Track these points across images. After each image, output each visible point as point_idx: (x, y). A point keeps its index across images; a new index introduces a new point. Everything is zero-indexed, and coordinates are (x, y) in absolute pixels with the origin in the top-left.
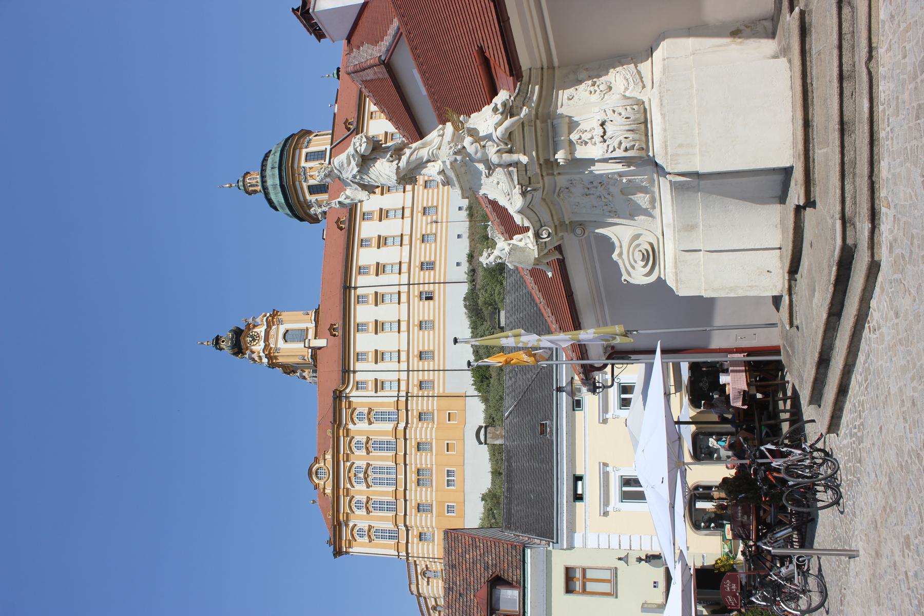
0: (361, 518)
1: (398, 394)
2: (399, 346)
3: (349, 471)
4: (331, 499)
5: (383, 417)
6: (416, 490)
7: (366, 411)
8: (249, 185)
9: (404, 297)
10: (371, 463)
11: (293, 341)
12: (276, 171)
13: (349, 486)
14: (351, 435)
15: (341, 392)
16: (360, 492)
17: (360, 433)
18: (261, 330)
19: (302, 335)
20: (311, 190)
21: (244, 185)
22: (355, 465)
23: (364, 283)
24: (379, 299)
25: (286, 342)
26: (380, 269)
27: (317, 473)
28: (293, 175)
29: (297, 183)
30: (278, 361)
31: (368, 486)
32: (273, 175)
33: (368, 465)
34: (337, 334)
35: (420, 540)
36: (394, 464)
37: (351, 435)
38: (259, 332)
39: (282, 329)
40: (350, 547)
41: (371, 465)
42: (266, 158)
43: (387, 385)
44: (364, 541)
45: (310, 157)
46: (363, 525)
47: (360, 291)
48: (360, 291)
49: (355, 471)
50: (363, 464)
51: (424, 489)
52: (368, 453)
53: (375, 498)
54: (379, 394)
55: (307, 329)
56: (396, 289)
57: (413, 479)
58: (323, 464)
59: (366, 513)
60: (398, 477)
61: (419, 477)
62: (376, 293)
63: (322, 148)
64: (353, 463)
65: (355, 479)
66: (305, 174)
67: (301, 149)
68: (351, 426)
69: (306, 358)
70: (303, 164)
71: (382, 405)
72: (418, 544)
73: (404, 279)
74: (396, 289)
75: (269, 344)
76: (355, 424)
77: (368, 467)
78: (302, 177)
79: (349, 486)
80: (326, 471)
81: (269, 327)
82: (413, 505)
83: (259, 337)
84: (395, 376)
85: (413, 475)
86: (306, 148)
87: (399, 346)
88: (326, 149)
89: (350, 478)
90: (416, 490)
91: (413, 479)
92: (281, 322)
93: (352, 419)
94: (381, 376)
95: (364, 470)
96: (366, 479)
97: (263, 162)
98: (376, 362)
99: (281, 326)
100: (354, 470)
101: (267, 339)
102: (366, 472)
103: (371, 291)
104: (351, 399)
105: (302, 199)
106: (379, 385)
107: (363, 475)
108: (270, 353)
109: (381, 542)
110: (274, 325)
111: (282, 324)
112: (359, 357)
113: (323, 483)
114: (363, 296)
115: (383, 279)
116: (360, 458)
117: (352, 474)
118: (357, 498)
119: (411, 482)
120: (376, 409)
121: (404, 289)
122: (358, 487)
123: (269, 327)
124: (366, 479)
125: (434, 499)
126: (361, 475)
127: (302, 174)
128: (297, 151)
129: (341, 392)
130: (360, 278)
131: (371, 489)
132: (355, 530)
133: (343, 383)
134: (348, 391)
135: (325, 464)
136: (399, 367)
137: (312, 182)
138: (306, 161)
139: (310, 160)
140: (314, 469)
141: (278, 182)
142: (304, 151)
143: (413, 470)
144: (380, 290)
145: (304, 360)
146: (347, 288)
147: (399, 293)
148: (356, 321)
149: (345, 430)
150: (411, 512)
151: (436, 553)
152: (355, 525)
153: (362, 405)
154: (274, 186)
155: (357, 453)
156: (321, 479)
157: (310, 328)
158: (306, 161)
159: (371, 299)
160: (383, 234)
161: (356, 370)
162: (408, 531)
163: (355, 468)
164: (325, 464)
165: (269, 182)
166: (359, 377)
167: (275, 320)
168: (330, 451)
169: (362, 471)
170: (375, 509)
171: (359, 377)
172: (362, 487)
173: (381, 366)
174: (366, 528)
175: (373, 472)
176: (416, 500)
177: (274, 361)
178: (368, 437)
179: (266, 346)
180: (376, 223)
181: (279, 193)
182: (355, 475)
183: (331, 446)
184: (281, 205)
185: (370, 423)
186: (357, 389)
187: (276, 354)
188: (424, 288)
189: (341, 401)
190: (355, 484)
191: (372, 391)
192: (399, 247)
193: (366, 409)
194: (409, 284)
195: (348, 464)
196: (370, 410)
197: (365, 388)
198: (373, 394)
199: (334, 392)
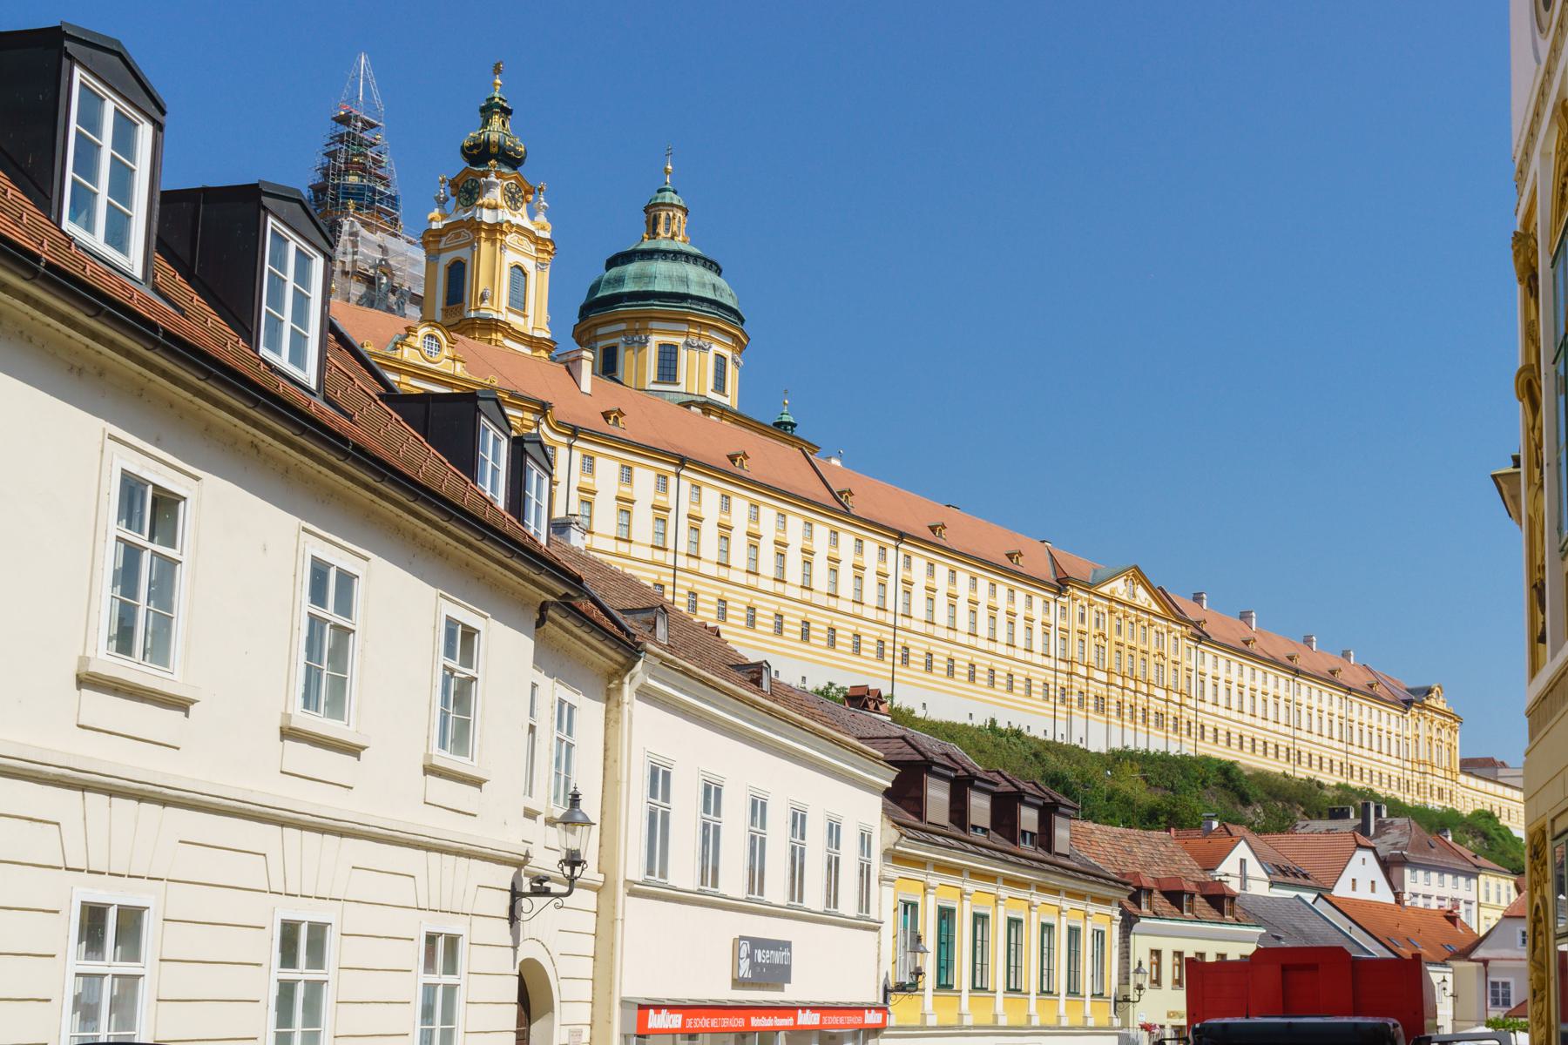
2: (599, 535)
4: (391, 354)
8: (671, 214)
9: (659, 556)
12: (710, 295)
15: (545, 416)
18: (521, 218)
19: (518, 303)
20: (668, 349)
21: (672, 205)
25: (512, 268)
27: (431, 336)
28: (701, 325)
29: (685, 328)
30: (482, 240)
32: (703, 285)
34: (611, 422)
38: (520, 211)
39: (529, 266)
42: (708, 264)
45: (720, 361)
47: (672, 480)
48: (672, 480)
55: (525, 316)
56: (670, 545)
62: (667, 510)
63: (728, 390)
66: (699, 347)
67: (733, 349)
69: (487, 304)
70: (716, 348)
73: (682, 562)
78: (694, 340)
81: (537, 240)
86: (733, 359)
87: (599, 535)
88: (727, 396)
92: (540, 266)
97: (716, 265)
98: (580, 489)
99: (534, 263)
101: (521, 230)
105: (654, 325)
108: (502, 232)
110: (538, 250)
111: (537, 266)
113: (418, 345)
115: (684, 524)
123: (537, 240)
127: (700, 343)
129: (545, 416)
133: (559, 423)
135: (447, 358)
137: (683, 354)
138: (716, 354)
139: (717, 362)
140: (439, 332)
141: (694, 291)
142: (728, 353)
144: (672, 514)
145: (483, 298)
146: (682, 461)
148: (637, 466)
154: (685, 280)
157: (526, 323)
158: (716, 354)
159: (661, 500)
164: (447, 358)
165: (694, 272)
167: (545, 255)
168: (466, 375)
173: (574, 494)
177: (483, 234)
179: (512, 226)
181: (673, 286)
183: (474, 378)
184: (647, 280)
187: (498, 245)
192: (716, 561)
199: (550, 406)
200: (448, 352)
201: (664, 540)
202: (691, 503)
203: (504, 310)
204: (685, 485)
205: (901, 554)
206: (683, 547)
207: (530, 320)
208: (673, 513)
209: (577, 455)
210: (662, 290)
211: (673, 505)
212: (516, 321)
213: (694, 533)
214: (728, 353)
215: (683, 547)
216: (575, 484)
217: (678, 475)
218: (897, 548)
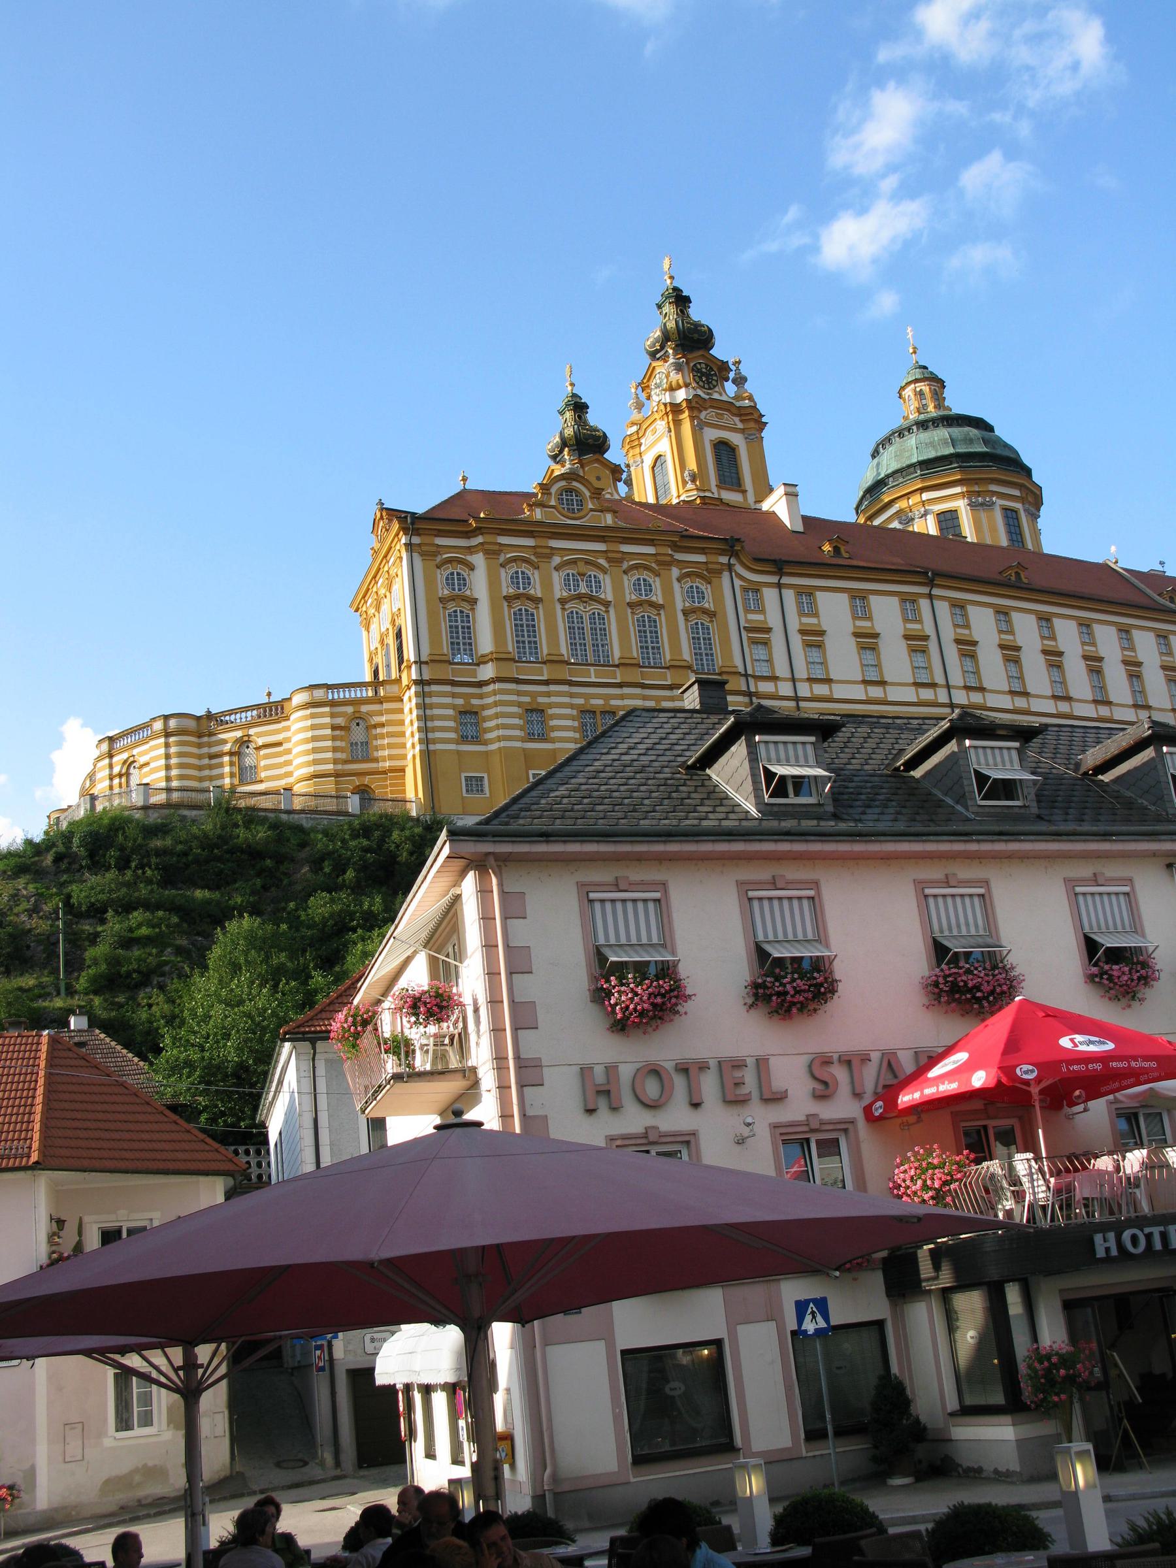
0: (493, 583)
1: (742, 675)
3: (588, 562)
5: (701, 641)
6: (572, 706)
7: (708, 604)
9: (927, 694)
10: (612, 610)
13: (557, 560)
14: (662, 572)
16: (547, 585)
17: (668, 591)
20: (948, 516)
22: (601, 576)
24: (916, 643)
31: (563, 601)
33: (607, 604)
35: (461, 713)
36: (617, 662)
37: (662, 572)
40: (422, 554)
41: (607, 612)
43: (760, 652)
44: (440, 586)
46: (479, 584)
47: (924, 604)
48: (924, 604)
49: (590, 576)
50: (608, 594)
51: (576, 724)
52: (630, 605)
53: (541, 614)
54: (744, 634)
55: (744, 492)
56: (940, 679)
57: (593, 702)
58: (591, 506)
59: (505, 594)
60: (592, 669)
61: (598, 714)
62: (926, 638)
64: (604, 571)
65: (573, 575)
67: (1022, 500)
68: (675, 572)
71: (726, 641)
72: (454, 707)
74: (940, 679)
75: (706, 409)
76: (679, 580)
77: (603, 605)
79: (557, 560)
80: (577, 515)
82: (541, 700)
83: (710, 389)
84: (782, 670)
85: (601, 702)
89: (574, 562)
90: (572, 706)
91: (593, 702)
93: (688, 575)
94: (777, 639)
95: (594, 594)
96: (580, 597)
100: (592, 573)
102: (592, 598)
103: (929, 630)
104: (726, 575)
106: (759, 634)
107: (583, 591)
109: (508, 622)
112: (806, 594)
113: (553, 503)
114: (917, 611)
115: (951, 652)
116: (618, 588)
117: (582, 567)
118: (535, 576)
119: (587, 697)
120: (713, 628)
122: (557, 578)
124: (580, 597)
125: (558, 745)
126: (583, 589)
128: (1017, 493)
131: (558, 607)
132: (460, 568)
134: (739, 569)
135: (592, 510)
136: (802, 680)
139: (1006, 517)
140: (575, 484)
142: (1018, 505)
143: (613, 702)
144: (933, 646)
149: (668, 559)
150: (525, 693)
151: (439, 746)
152: (472, 568)
153: (719, 598)
155: (628, 582)
156: (560, 500)
157: (745, 499)
161: (783, 591)
162: (481, 684)
163: (595, 577)
166: (770, 595)
169: (592, 591)
170: (518, 615)
171: (770, 595)
172: (559, 592)
173: (796, 641)
174: (468, 593)
175: (594, 614)
176: (551, 705)
178: (661, 607)
180: (1038, 645)
182: (582, 575)
185: (685, 613)
186: (745, 590)
189: (722, 552)
190: (563, 574)
191: (747, 621)
193: (712, 605)
195: (602, 561)
196: (712, 615)
197: (747, 610)
198: (743, 624)
199: (738, 540)
200: (593, 505)
201: (931, 672)
202: (956, 626)
203: (714, 489)
204: (943, 608)
209: (789, 595)
210: (925, 458)
211: (929, 630)
212: (729, 496)
213: (968, 663)
214: (1018, 505)
215: (956, 679)
216: (794, 623)
217: (930, 597)
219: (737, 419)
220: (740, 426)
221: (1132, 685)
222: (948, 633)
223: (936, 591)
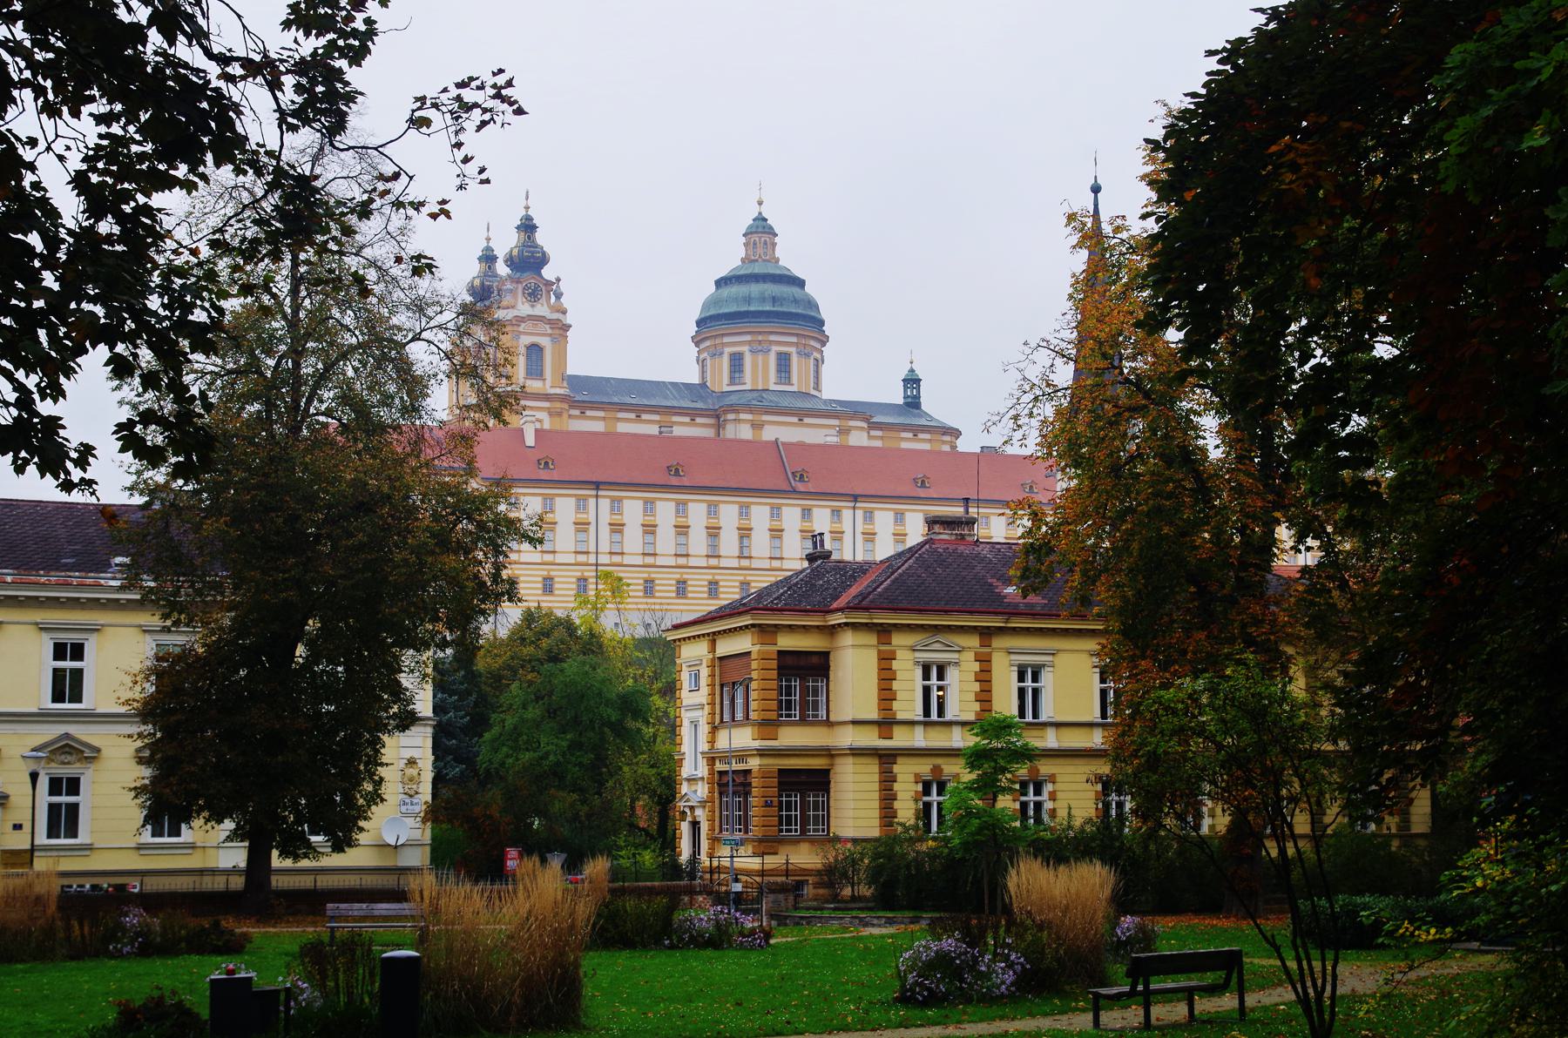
9: (582, 558)
11: (528, 357)
23: (601, 508)
26: (617, 528)
47: (592, 501)
48: (592, 501)
62: (589, 524)
63: (795, 379)
67: (796, 345)
74: (592, 548)
101: (531, 318)
115: (605, 531)
121: (592, 559)
128: (794, 339)
130: (608, 501)
142: (792, 350)
144: (592, 528)
146: (597, 485)
147: (587, 553)
160: (658, 530)
188: (592, 583)
194: (597, 565)
204: (605, 504)
205: (859, 513)
206: (605, 546)
207: (548, 382)
208: (594, 523)
211: (592, 519)
215: (605, 546)
218: (854, 508)
219: (547, 327)
220: (549, 331)
221: (741, 542)
222: (606, 517)
223: (600, 493)
